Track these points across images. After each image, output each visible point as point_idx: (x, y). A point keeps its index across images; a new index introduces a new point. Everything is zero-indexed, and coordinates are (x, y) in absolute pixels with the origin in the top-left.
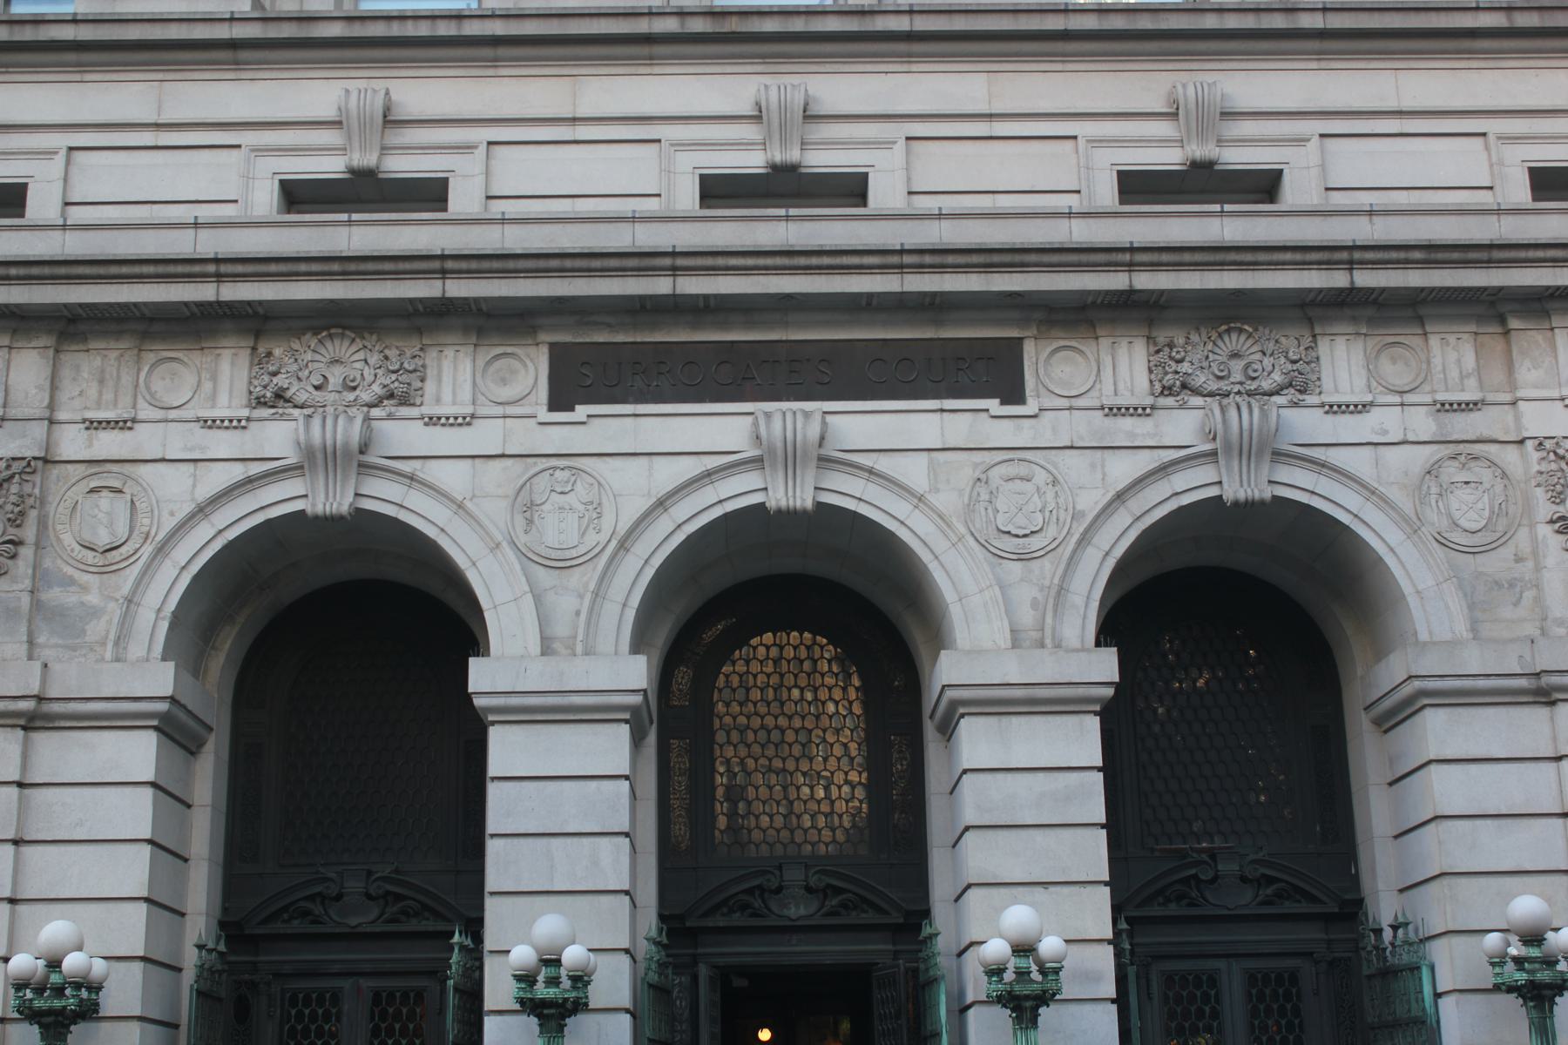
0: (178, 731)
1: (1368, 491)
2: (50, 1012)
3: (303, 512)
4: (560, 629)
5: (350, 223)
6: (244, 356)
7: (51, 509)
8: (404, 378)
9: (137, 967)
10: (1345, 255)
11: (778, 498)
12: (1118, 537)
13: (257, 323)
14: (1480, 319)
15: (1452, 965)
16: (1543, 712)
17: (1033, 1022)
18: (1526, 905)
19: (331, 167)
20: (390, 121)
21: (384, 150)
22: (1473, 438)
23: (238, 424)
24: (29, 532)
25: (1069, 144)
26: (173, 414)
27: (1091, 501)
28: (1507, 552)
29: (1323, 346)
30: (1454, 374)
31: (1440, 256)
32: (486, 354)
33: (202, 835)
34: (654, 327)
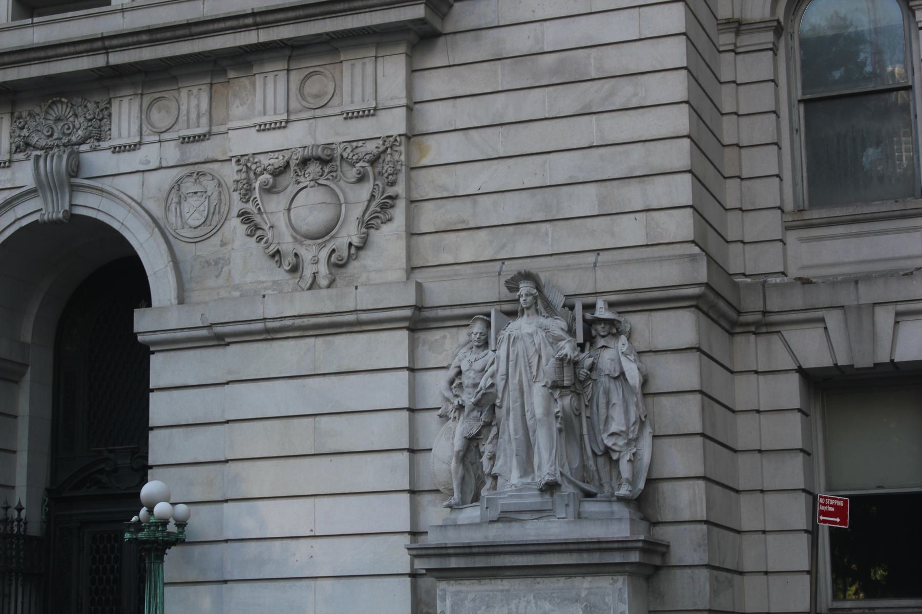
10: (99, 44)
22: (203, 160)
28: (216, 240)
30: (193, 115)
31: (159, 36)
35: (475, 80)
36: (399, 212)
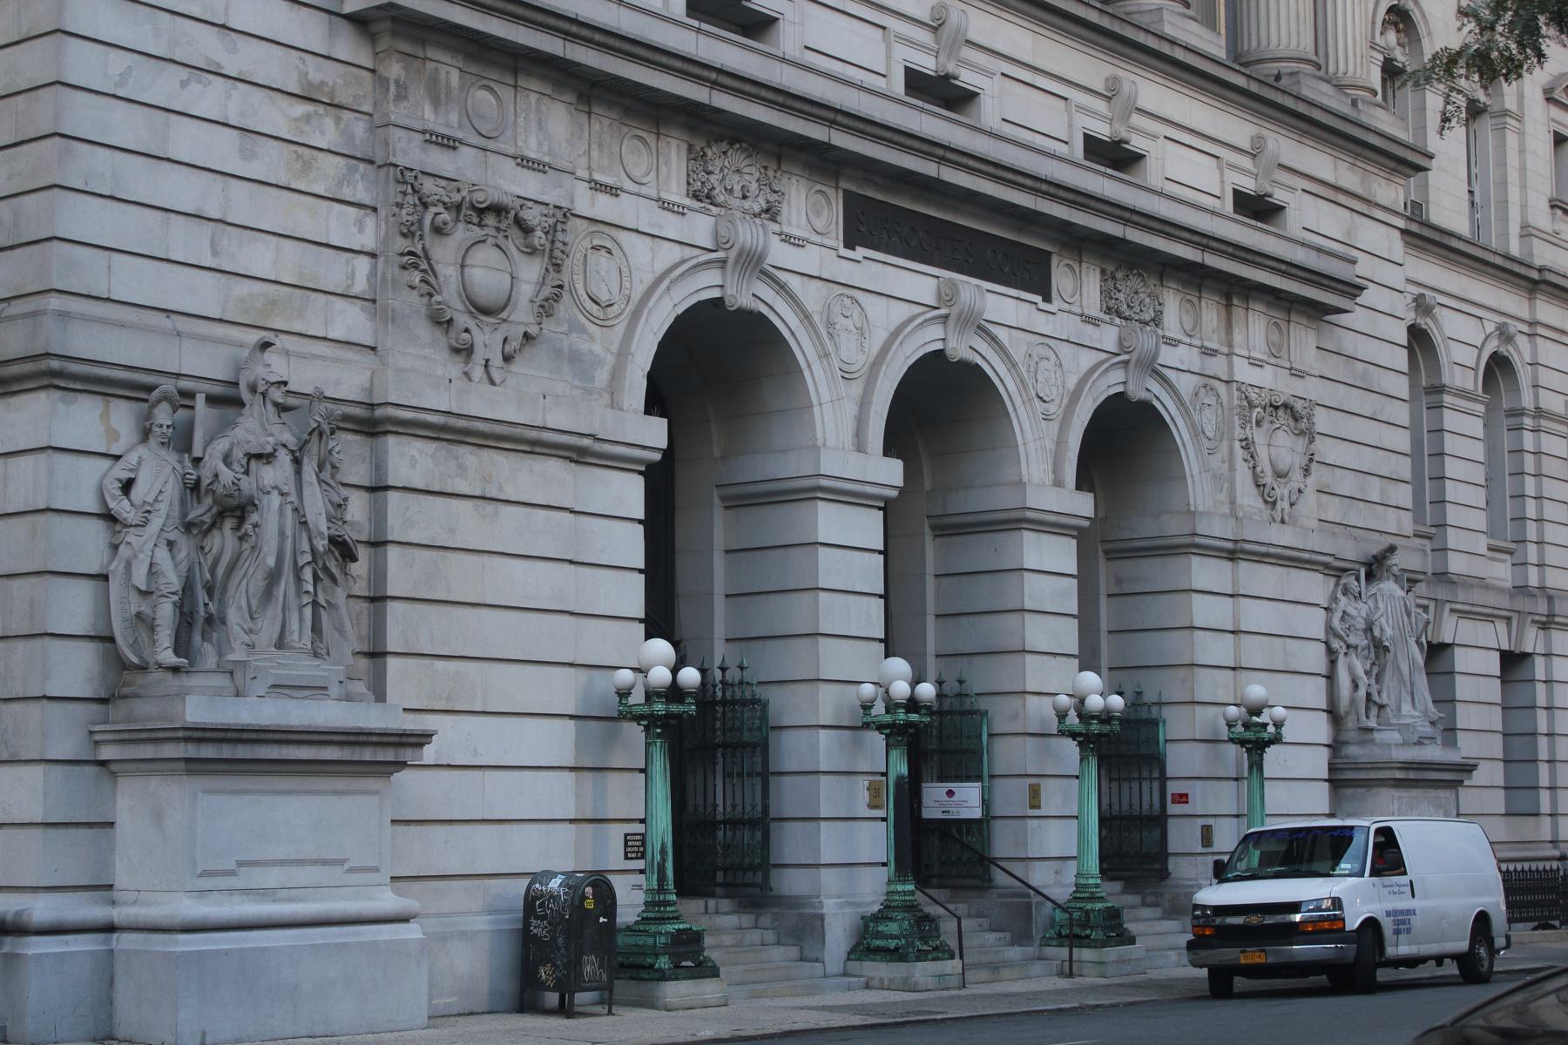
1: (806, 317)
16: (1227, 565)
18: (1256, 690)
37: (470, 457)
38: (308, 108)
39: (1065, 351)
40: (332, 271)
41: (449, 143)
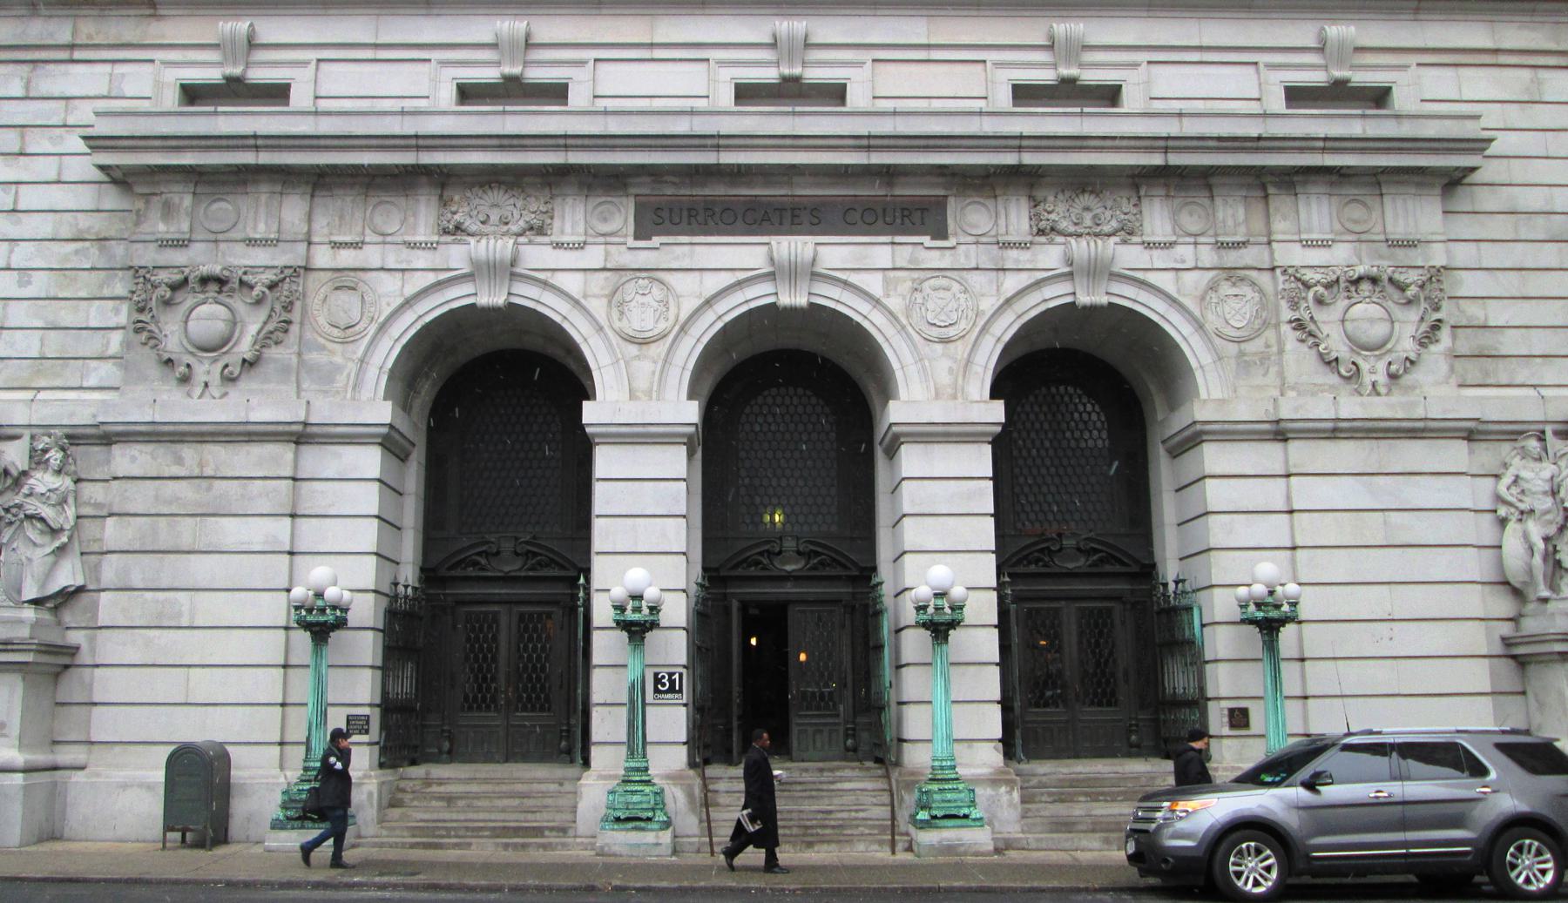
0: (392, 444)
2: (318, 624)
3: (473, 305)
4: (642, 383)
5: (504, 112)
6: (434, 200)
7: (309, 301)
8: (542, 217)
9: (371, 596)
11: (785, 300)
12: (1006, 327)
13: (443, 180)
14: (1249, 186)
15: (1221, 605)
17: (946, 638)
19: (490, 75)
20: (529, 45)
21: (526, 64)
23: (431, 247)
24: (296, 316)
25: (980, 67)
26: (389, 239)
27: (988, 305)
29: (1145, 203)
32: (593, 201)
33: (411, 513)
34: (703, 185)
35: (1499, 227)
36: (1445, 335)
37: (188, 452)
38: (79, 245)
39: (976, 279)
40: (92, 344)
41: (181, 244)
